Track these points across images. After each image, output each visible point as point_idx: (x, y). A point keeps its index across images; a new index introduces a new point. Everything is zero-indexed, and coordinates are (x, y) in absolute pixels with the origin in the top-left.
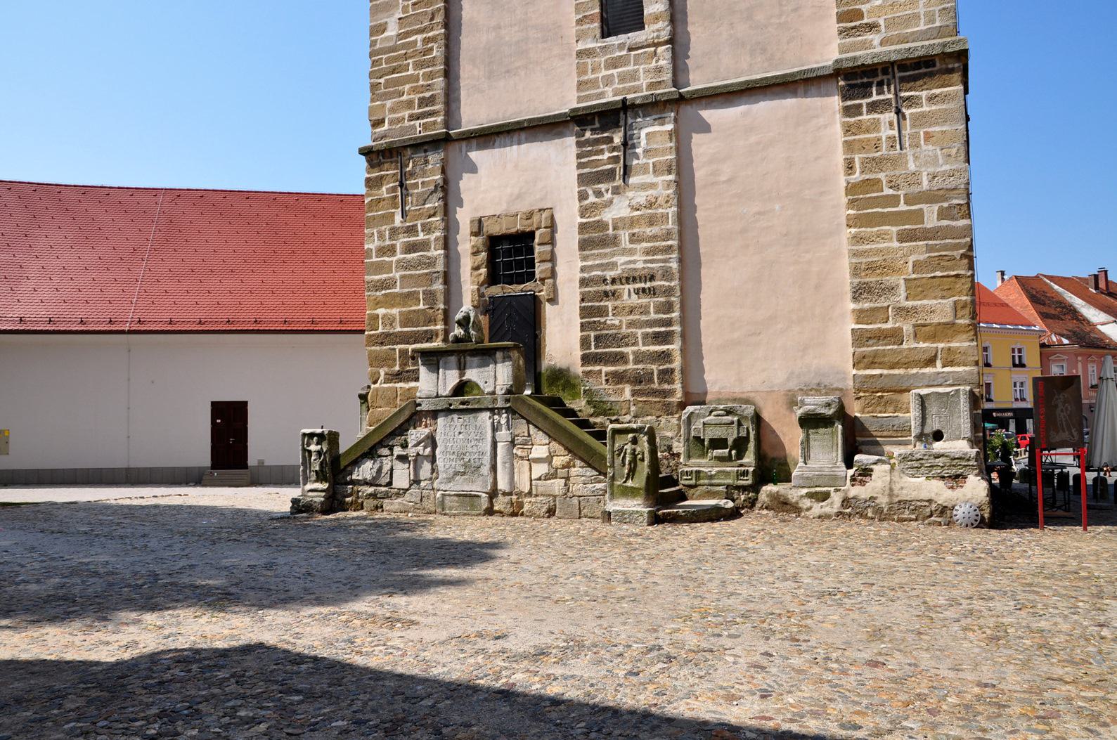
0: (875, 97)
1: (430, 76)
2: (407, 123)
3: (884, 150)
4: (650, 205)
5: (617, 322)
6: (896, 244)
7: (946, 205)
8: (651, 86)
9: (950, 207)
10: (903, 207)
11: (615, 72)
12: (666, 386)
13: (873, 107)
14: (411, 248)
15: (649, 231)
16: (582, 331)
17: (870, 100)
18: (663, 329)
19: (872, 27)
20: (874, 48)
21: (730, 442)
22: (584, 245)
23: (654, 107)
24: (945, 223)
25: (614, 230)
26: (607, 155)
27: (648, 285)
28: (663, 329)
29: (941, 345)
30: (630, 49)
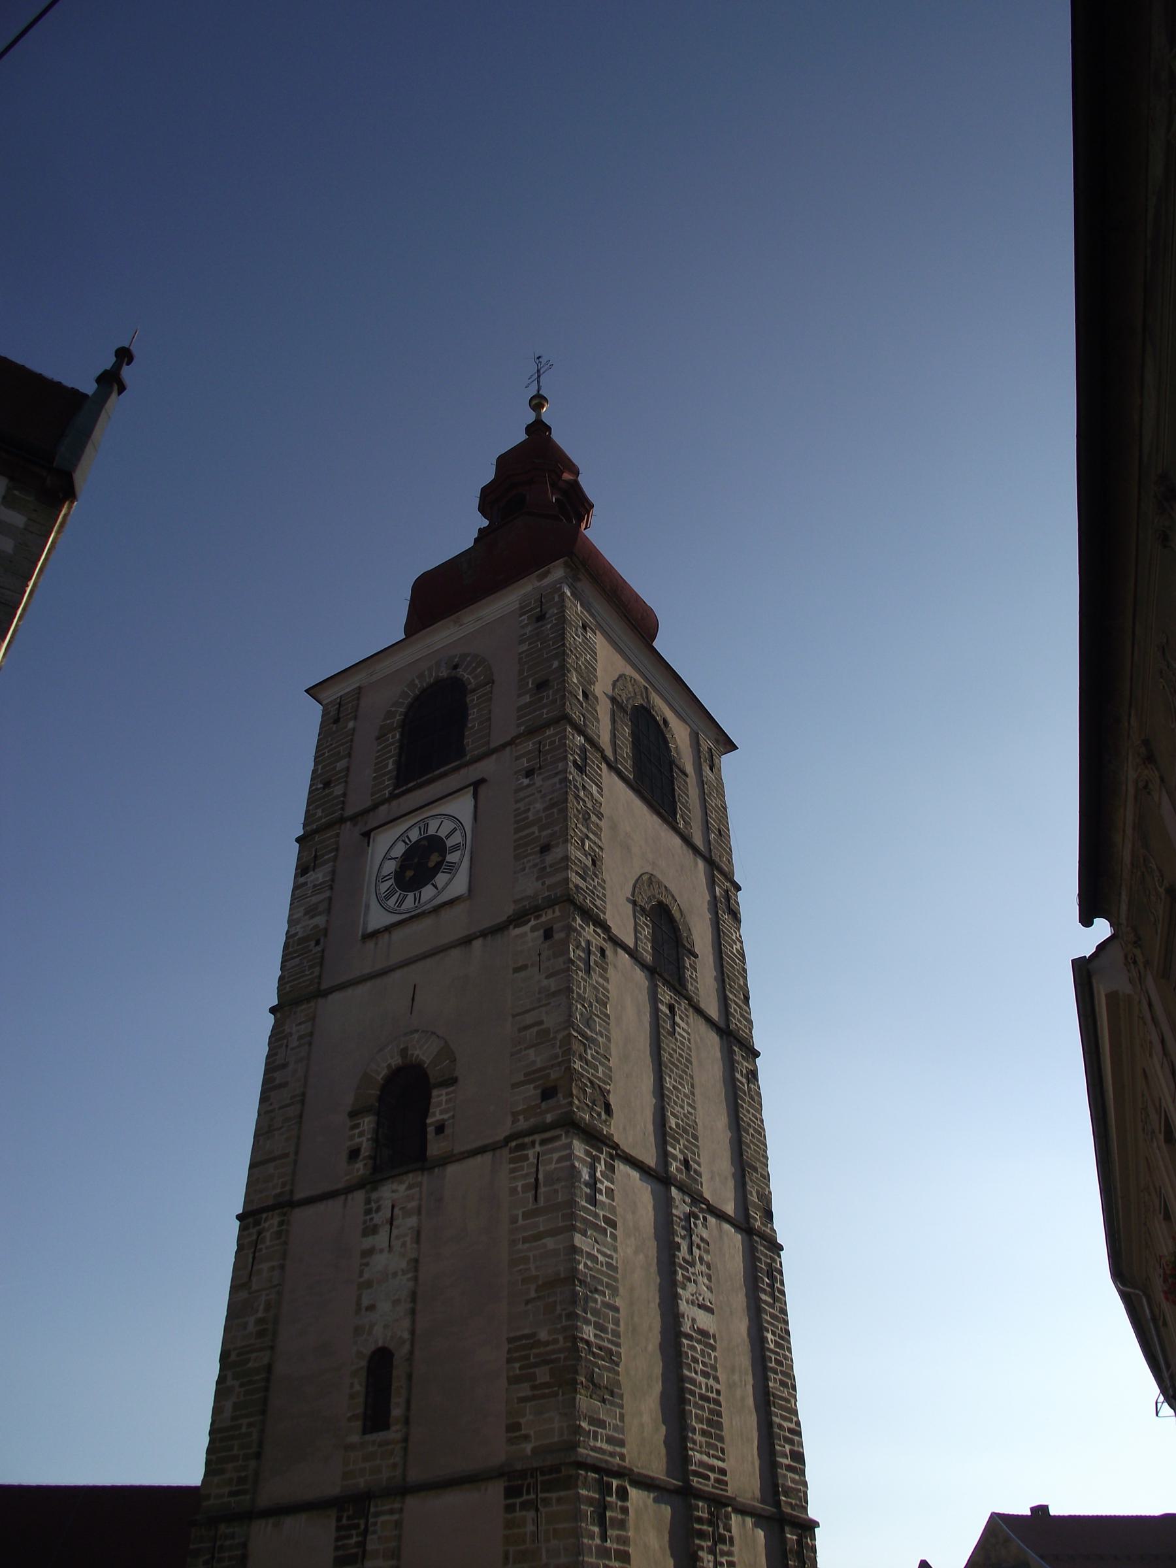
0: (525, 1497)
13: (525, 1506)
17: (521, 1500)
19: (526, 1438)
26: (354, 1540)
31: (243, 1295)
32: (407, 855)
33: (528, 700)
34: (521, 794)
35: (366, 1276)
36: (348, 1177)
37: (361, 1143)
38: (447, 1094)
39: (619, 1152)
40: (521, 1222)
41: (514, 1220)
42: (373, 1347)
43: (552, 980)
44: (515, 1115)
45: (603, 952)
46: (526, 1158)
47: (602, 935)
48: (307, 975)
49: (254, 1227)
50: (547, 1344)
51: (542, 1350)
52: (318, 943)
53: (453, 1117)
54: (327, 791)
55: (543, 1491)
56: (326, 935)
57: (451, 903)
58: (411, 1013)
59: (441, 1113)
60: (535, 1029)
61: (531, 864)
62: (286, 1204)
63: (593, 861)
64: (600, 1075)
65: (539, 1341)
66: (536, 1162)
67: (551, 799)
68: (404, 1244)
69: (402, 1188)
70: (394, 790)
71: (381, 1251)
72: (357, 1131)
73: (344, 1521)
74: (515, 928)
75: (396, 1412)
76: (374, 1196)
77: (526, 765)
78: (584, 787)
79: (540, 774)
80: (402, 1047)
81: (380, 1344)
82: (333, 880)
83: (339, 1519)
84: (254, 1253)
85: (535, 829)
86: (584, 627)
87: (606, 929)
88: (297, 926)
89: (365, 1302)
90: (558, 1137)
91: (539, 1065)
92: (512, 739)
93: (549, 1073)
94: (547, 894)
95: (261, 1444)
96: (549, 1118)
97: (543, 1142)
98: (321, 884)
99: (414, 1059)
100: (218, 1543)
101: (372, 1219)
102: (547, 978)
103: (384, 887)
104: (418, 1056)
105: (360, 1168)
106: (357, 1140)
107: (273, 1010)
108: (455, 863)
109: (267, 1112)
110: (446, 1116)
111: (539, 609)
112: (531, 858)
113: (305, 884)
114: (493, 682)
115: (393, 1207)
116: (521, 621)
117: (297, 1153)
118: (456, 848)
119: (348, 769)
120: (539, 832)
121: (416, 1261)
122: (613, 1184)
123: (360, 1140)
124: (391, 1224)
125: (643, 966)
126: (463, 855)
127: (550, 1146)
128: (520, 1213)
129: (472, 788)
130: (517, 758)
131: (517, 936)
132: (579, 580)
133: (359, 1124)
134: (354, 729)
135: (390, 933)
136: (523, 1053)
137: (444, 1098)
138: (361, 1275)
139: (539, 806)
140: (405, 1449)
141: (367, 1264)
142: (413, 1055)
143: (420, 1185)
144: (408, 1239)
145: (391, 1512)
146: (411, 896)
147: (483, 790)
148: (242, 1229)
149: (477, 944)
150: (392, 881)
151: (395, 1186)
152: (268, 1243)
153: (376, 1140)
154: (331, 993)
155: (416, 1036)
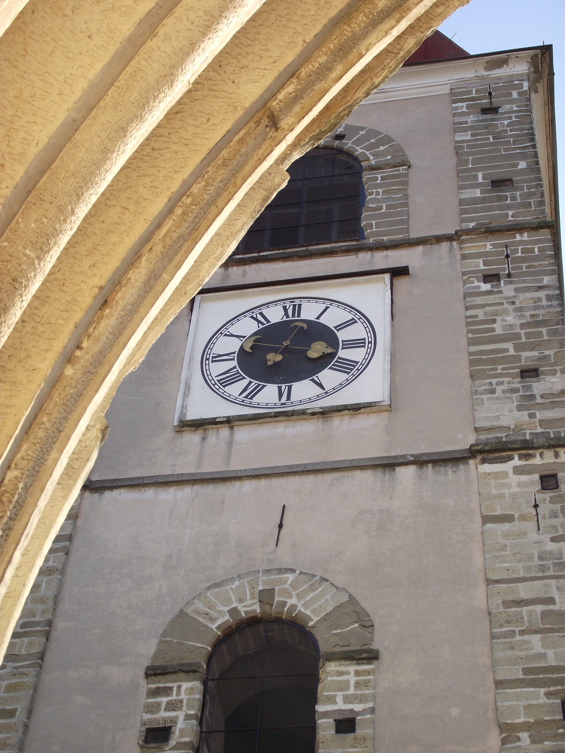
37: (174, 721)
38: (357, 673)
53: (372, 710)
57: (356, 409)
58: (276, 546)
59: (347, 700)
60: (539, 608)
72: (164, 700)
74: (483, 461)
80: (260, 588)
85: (509, 346)
92: (456, 232)
99: (286, 609)
104: (294, 607)
106: (163, 714)
108: (357, 363)
110: (358, 707)
112: (506, 380)
114: (409, 167)
116: (457, 108)
117: (30, 713)
132: (536, 92)
133: (171, 689)
135: (232, 428)
142: (285, 603)
154: (111, 488)
155: (290, 577)
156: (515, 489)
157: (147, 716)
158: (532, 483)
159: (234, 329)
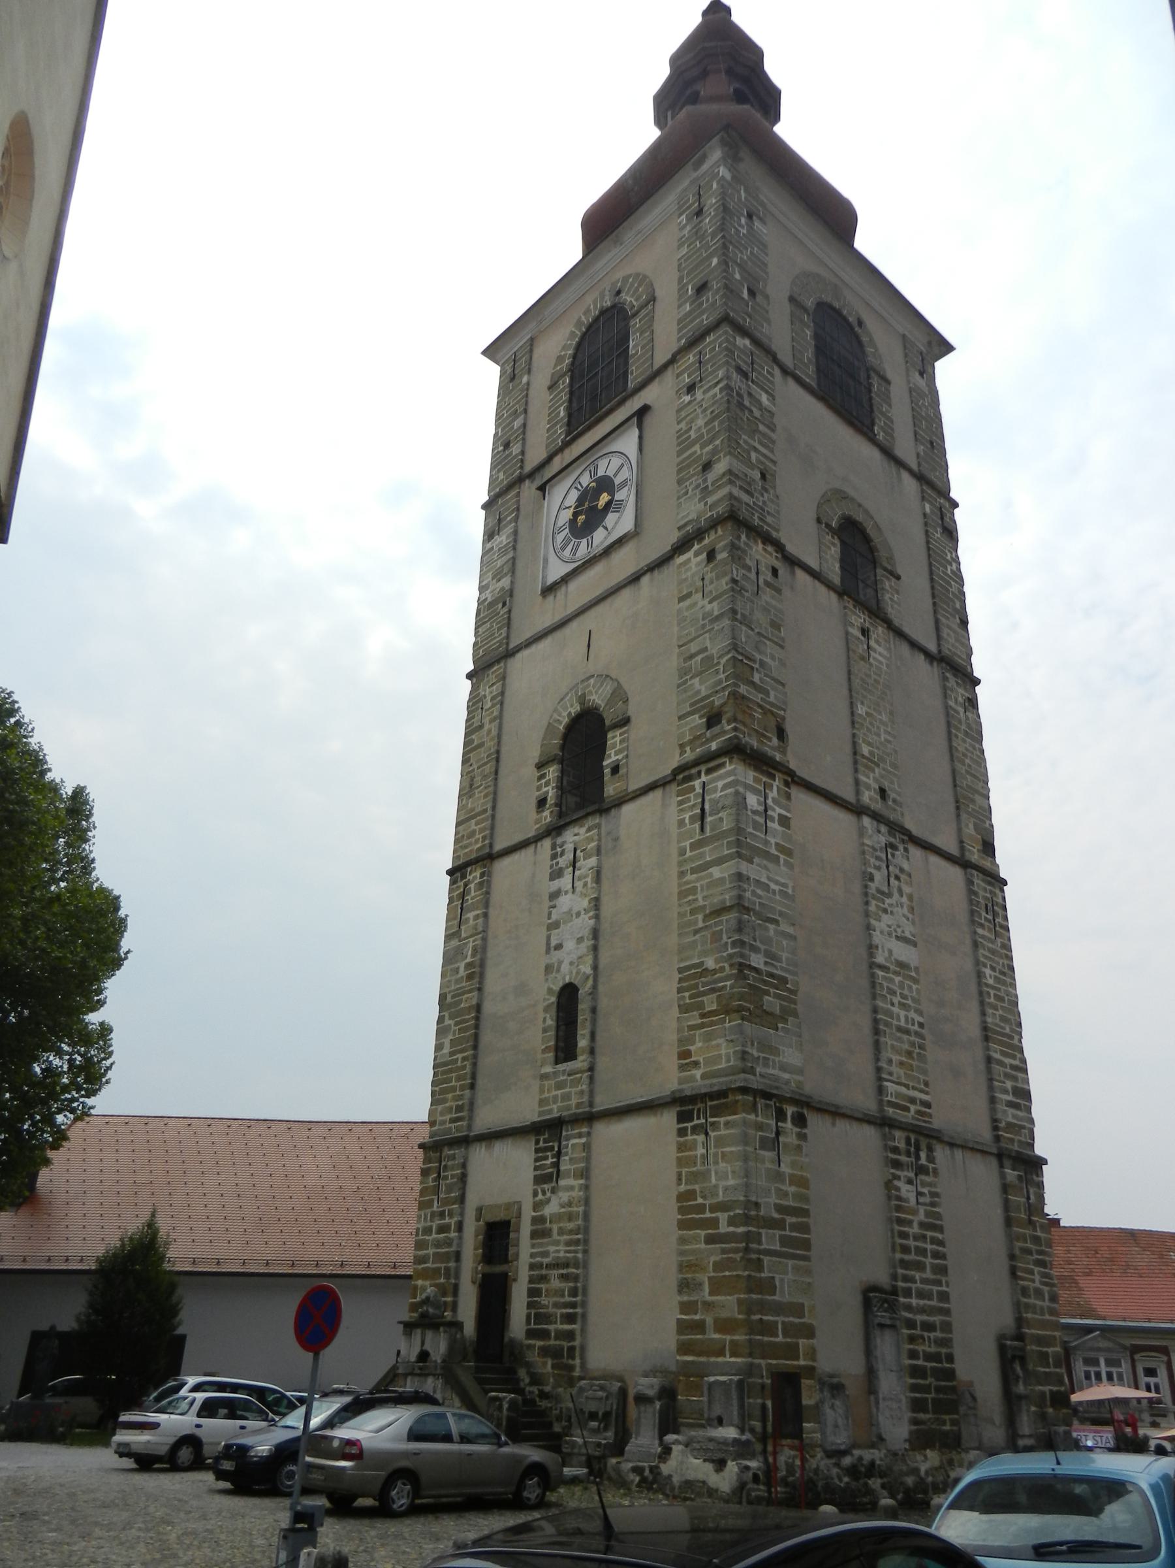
0: (696, 1122)
1: (462, 1088)
2: (448, 1125)
3: (699, 1167)
4: (570, 1204)
5: (546, 1303)
6: (703, 1246)
7: (732, 1214)
8: (578, 1105)
9: (735, 1215)
10: (708, 1215)
11: (559, 1092)
12: (571, 1362)
13: (695, 1130)
14: (443, 1229)
15: (571, 1226)
16: (528, 1308)
18: (571, 1311)
19: (696, 1064)
20: (698, 1081)
21: (600, 1414)
22: (534, 1235)
23: (576, 1120)
24: (732, 1229)
25: (550, 1222)
26: (550, 1161)
27: (564, 1271)
28: (571, 1311)
29: (728, 1337)
30: (569, 1075)
31: (455, 943)
32: (580, 501)
33: (688, 309)
34: (683, 414)
35: (554, 917)
36: (538, 826)
37: (547, 792)
38: (621, 735)
39: (796, 779)
40: (688, 854)
41: (682, 852)
42: (561, 984)
43: (715, 604)
44: (682, 746)
45: (775, 572)
46: (693, 789)
47: (775, 554)
48: (495, 638)
49: (461, 880)
50: (715, 971)
51: (709, 978)
52: (504, 604)
53: (627, 756)
54: (507, 452)
55: (712, 1116)
56: (511, 596)
57: (620, 542)
59: (616, 754)
60: (699, 658)
61: (692, 486)
62: (488, 858)
63: (763, 476)
64: (772, 699)
65: (706, 969)
66: (701, 791)
67: (712, 412)
68: (585, 884)
69: (583, 830)
70: (566, 437)
71: (566, 892)
72: (543, 781)
73: (541, 1144)
75: (583, 1043)
76: (559, 841)
77: (687, 381)
78: (750, 394)
79: (701, 387)
81: (567, 981)
82: (515, 541)
83: (537, 1142)
84: (462, 904)
85: (697, 448)
86: (750, 216)
87: (779, 547)
88: (488, 592)
89: (553, 943)
90: (722, 765)
91: (703, 693)
93: (714, 701)
94: (709, 514)
95: (474, 1076)
96: (714, 746)
97: (709, 772)
98: (505, 546)
100: (443, 1163)
101: (557, 863)
102: (710, 602)
103: (560, 538)
105: (547, 816)
106: (545, 789)
107: (470, 676)
109: (469, 773)
110: (620, 757)
111: (697, 204)
112: (693, 479)
113: (492, 549)
115: (575, 850)
117: (494, 808)
118: (624, 484)
119: (524, 425)
120: (701, 448)
121: (597, 899)
122: (788, 811)
123: (546, 789)
124: (574, 867)
125: (829, 586)
126: (630, 491)
127: (715, 774)
128: (687, 844)
129: (636, 418)
130: (678, 376)
131: (681, 564)
132: (741, 160)
134: (528, 384)
136: (689, 683)
137: (618, 739)
138: (550, 914)
139: (700, 422)
140: (591, 1078)
141: (554, 907)
143: (598, 826)
144: (589, 879)
145: (580, 1136)
146: (584, 541)
147: (648, 420)
148: (452, 883)
149: (645, 580)
150: (567, 530)
151: (576, 830)
152: (473, 894)
153: (560, 788)
154: (518, 651)
155: (592, 681)
156: (694, 569)
157: (538, 793)
158: (701, 562)
159: (567, 504)
